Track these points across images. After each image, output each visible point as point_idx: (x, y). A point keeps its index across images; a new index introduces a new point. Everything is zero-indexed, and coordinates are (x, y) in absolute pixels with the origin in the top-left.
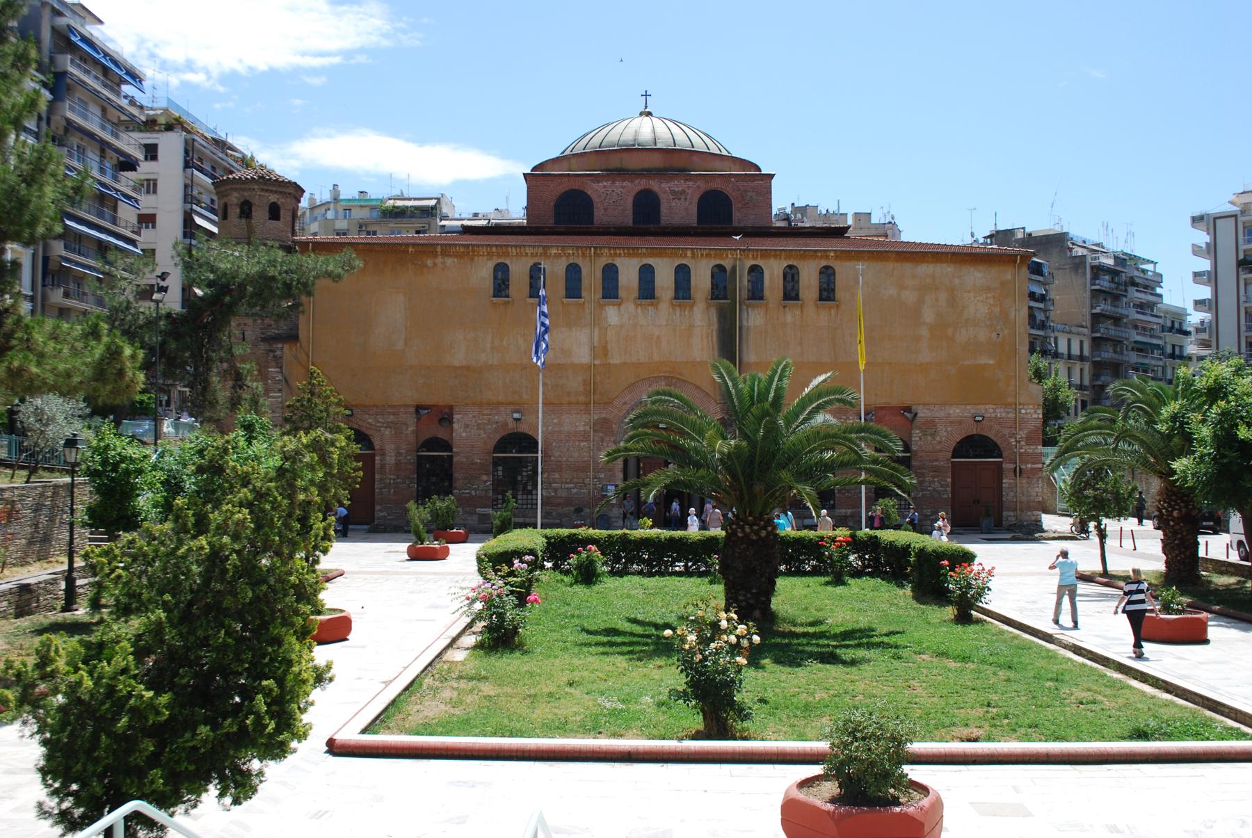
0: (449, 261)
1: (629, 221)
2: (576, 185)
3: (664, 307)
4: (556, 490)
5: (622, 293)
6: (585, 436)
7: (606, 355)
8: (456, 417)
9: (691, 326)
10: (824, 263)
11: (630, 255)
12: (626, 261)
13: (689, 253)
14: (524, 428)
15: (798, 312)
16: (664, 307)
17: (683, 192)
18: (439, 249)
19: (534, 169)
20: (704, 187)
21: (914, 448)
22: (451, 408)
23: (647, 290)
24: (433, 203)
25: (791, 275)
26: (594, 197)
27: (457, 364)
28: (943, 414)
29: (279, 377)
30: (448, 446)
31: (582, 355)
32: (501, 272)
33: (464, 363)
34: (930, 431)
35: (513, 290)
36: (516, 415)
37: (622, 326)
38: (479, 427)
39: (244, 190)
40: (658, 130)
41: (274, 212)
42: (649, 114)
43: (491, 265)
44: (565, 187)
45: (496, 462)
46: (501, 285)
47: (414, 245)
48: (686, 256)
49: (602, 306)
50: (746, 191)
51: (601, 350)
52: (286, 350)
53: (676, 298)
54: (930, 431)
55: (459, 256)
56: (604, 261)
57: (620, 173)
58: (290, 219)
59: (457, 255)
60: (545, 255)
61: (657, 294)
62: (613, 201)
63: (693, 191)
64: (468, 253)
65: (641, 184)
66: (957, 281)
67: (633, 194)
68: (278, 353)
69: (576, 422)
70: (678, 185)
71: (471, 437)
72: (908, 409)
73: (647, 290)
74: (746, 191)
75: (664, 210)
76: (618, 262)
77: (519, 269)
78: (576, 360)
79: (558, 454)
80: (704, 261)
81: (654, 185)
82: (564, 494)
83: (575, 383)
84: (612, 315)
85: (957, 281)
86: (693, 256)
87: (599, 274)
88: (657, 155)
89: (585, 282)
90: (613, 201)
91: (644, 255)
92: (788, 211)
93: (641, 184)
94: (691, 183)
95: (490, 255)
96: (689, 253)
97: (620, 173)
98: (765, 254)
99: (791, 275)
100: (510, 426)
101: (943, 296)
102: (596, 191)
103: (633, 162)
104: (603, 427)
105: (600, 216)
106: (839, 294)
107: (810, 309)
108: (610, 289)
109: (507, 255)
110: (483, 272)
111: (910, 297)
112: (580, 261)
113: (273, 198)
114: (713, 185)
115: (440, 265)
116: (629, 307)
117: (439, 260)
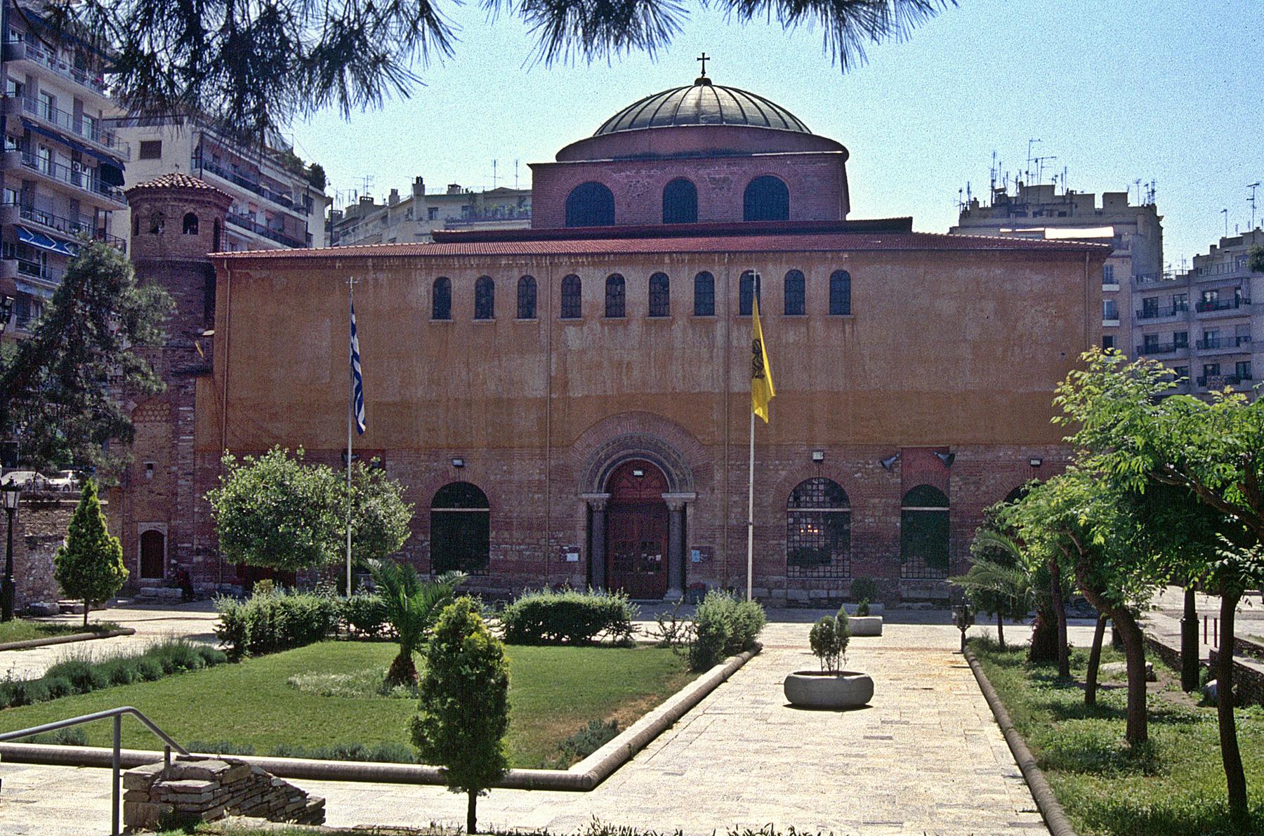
0: (383, 277)
1: (657, 218)
2: (592, 175)
3: (636, 328)
4: (505, 553)
5: (585, 311)
6: (540, 486)
7: (565, 385)
10: (834, 267)
11: (594, 264)
13: (667, 260)
14: (466, 477)
15: (803, 329)
16: (636, 328)
17: (725, 180)
18: (370, 262)
21: (953, 500)
25: (795, 283)
27: (390, 399)
28: (989, 456)
29: (190, 417)
31: (536, 387)
33: (398, 399)
34: (973, 479)
35: (455, 310)
37: (584, 351)
39: (156, 200)
40: (704, 103)
41: (190, 223)
46: (442, 303)
47: (341, 258)
48: (663, 263)
50: (806, 176)
51: (557, 382)
52: (200, 386)
53: (652, 314)
54: (973, 479)
56: (563, 272)
57: (649, 159)
58: (210, 232)
59: (390, 268)
61: (628, 309)
62: (639, 192)
63: (738, 176)
65: (673, 172)
66: (1008, 286)
67: (663, 184)
68: (190, 389)
69: (528, 470)
70: (720, 170)
72: (945, 450)
74: (806, 176)
75: (702, 204)
78: (529, 393)
79: (506, 508)
81: (690, 172)
83: (526, 421)
84: (573, 336)
85: (1008, 286)
86: (672, 260)
87: (557, 289)
89: (541, 298)
90: (639, 192)
91: (614, 263)
93: (673, 172)
94: (735, 169)
95: (429, 269)
96: (667, 260)
97: (649, 159)
98: (761, 255)
99: (795, 283)
100: (451, 474)
101: (990, 306)
102: (617, 181)
103: (666, 145)
104: (561, 476)
105: (623, 214)
106: (856, 306)
107: (818, 326)
108: (571, 306)
111: (947, 307)
113: (189, 209)
114: (764, 170)
115: (371, 282)
117: (371, 275)
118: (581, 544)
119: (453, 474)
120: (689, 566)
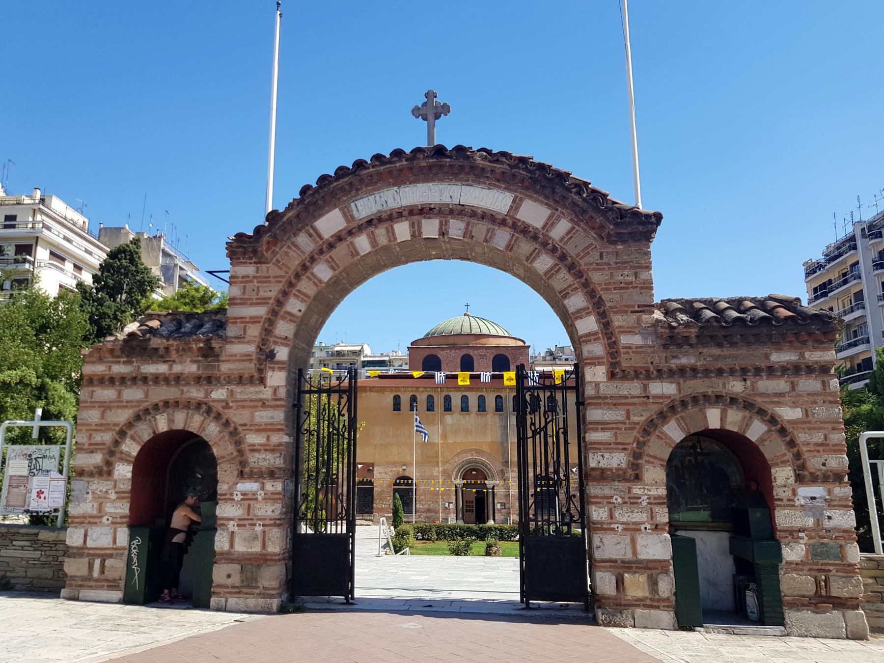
0: (373, 394)
2: (433, 352)
8: (375, 469)
9: (486, 424)
12: (455, 393)
14: (406, 474)
19: (412, 344)
20: (495, 352)
22: (373, 465)
23: (465, 408)
24: (359, 348)
26: (441, 358)
30: (371, 483)
32: (397, 399)
36: (404, 468)
38: (386, 473)
42: (468, 315)
43: (392, 396)
44: (427, 353)
45: (395, 491)
46: (397, 406)
49: (444, 415)
55: (378, 392)
56: (444, 394)
59: (376, 391)
60: (417, 391)
64: (382, 390)
71: (382, 479)
73: (465, 408)
76: (451, 394)
77: (405, 398)
80: (492, 394)
82: (426, 507)
84: (449, 419)
88: (472, 337)
92: (553, 349)
95: (392, 391)
102: (441, 355)
103: (460, 341)
108: (448, 408)
109: (399, 391)
110: (389, 399)
112: (433, 394)
114: (500, 352)
116: (458, 415)
117: (368, 393)
118: (454, 501)
119: (401, 474)
120: (496, 511)
